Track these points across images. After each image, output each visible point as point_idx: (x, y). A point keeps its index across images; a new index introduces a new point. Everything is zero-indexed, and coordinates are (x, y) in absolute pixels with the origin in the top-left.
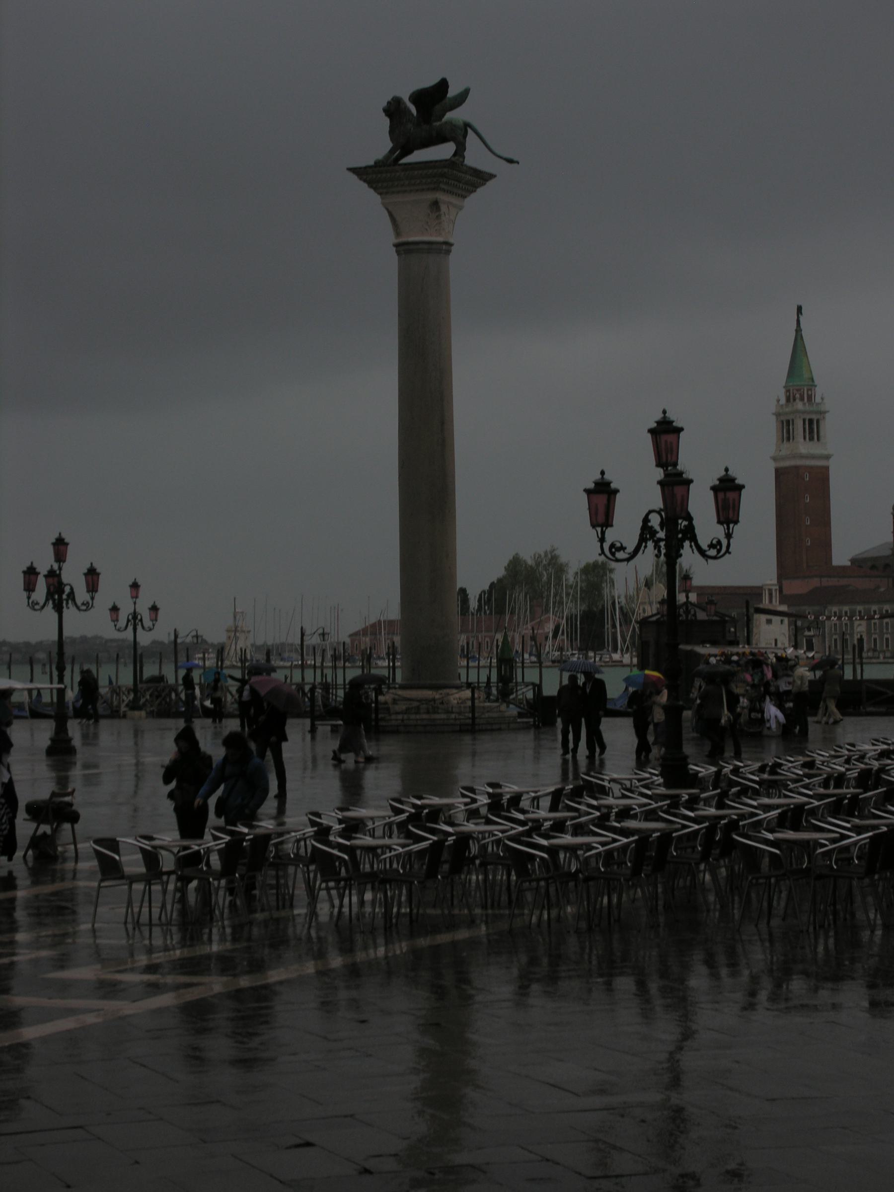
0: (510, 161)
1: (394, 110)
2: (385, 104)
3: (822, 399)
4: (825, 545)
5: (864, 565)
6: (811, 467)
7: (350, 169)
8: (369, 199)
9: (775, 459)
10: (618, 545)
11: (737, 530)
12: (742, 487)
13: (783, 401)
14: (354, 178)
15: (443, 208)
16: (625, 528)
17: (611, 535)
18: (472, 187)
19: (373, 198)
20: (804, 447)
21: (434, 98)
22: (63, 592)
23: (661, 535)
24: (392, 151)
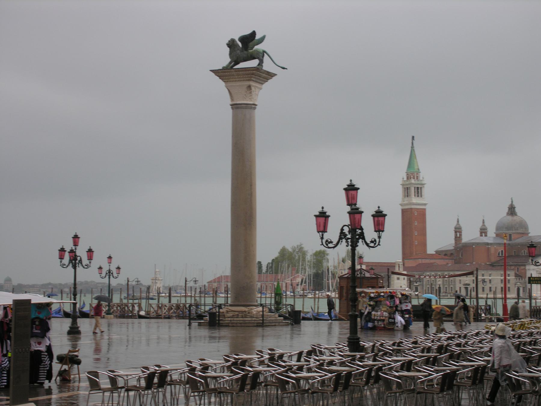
0: (284, 68)
1: (231, 44)
2: (227, 42)
4: (424, 244)
5: (441, 254)
7: (211, 71)
8: (220, 84)
9: (401, 205)
10: (329, 241)
11: (383, 234)
12: (385, 215)
13: (405, 179)
14: (213, 74)
15: (253, 88)
16: (333, 234)
17: (326, 236)
18: (267, 79)
20: (415, 200)
21: (249, 40)
22: (76, 259)
23: (349, 236)
24: (230, 63)
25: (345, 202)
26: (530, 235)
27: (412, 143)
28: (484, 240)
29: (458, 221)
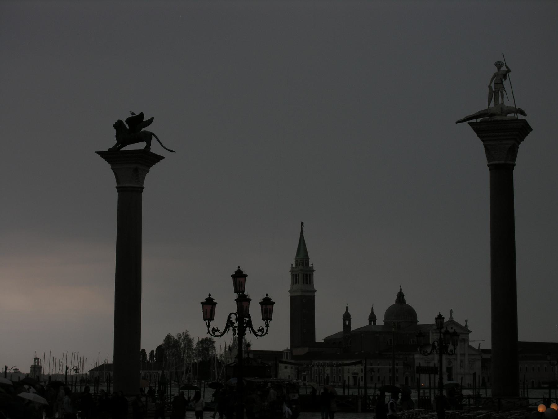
1: (118, 126)
3: (312, 264)
5: (330, 341)
7: (97, 152)
9: (289, 291)
11: (271, 323)
13: (294, 266)
16: (219, 322)
17: (213, 324)
18: (154, 163)
19: (107, 166)
23: (236, 324)
24: (117, 145)
25: (234, 291)
26: (418, 323)
27: (302, 229)
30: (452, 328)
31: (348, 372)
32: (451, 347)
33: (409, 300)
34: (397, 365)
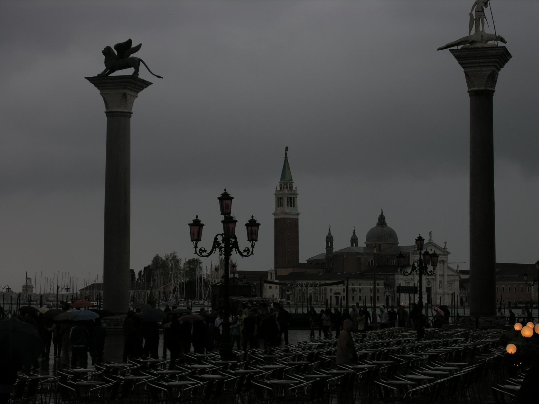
0: (159, 77)
1: (107, 52)
3: (296, 188)
4: (296, 253)
5: (312, 263)
6: (290, 219)
9: (274, 214)
10: (203, 249)
11: (256, 244)
13: (279, 189)
15: (128, 97)
16: (206, 243)
17: (200, 245)
19: (97, 91)
20: (287, 209)
21: (126, 48)
23: (223, 245)
24: (106, 71)
25: (220, 213)
26: (399, 245)
27: (286, 154)
28: (355, 250)
29: (330, 231)
30: (431, 250)
31: (331, 292)
32: (430, 268)
33: (390, 222)
34: (378, 285)
